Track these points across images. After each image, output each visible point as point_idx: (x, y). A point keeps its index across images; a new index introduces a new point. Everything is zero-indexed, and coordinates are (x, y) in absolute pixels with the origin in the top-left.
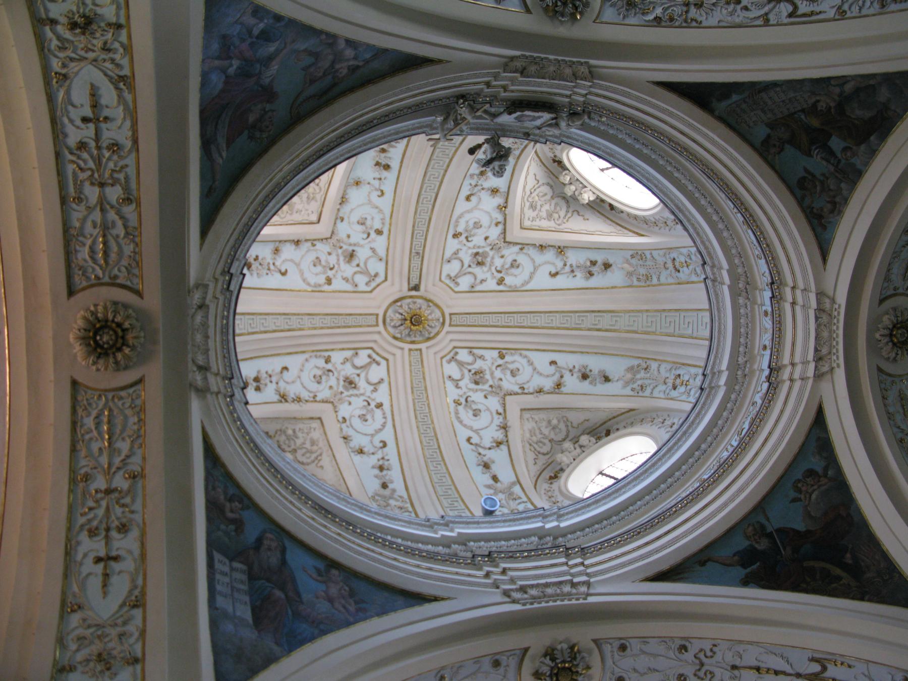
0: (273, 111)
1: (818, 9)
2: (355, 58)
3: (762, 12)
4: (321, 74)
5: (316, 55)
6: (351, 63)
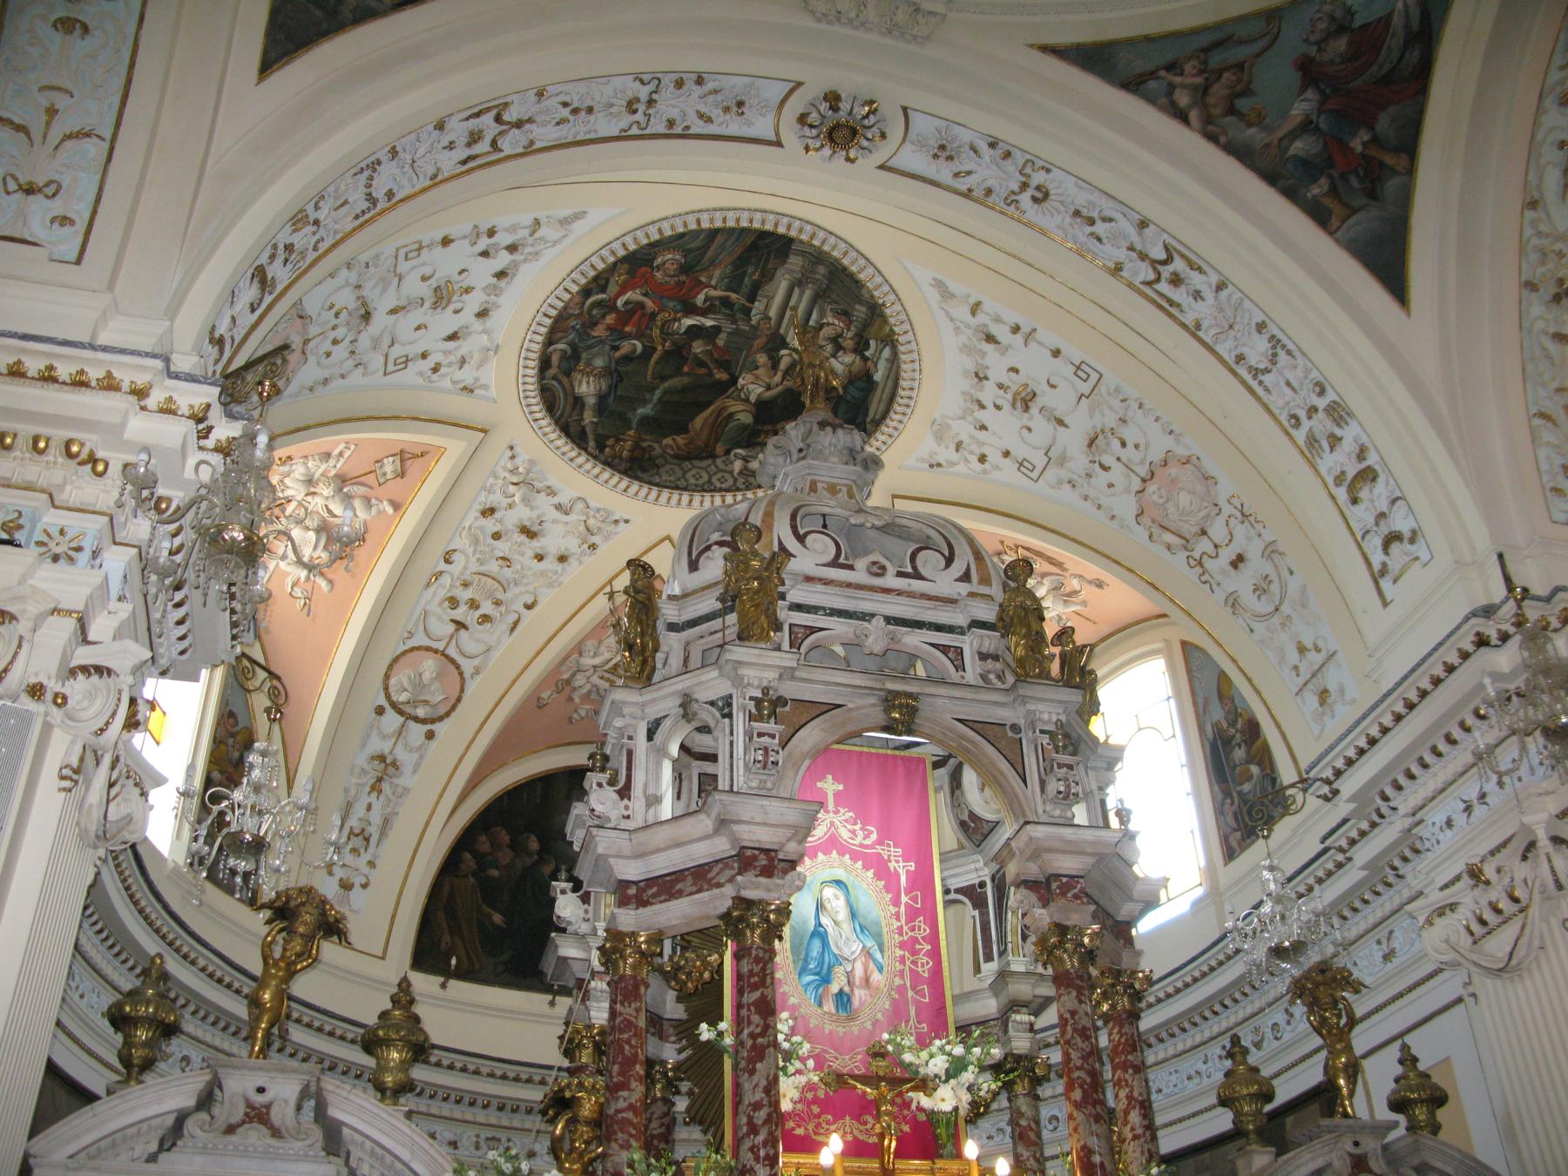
0: (1306, 40)
1: (473, 122)
2: (1171, 88)
3: (546, 103)
4: (1226, 75)
5: (1231, 110)
6: (1178, 80)
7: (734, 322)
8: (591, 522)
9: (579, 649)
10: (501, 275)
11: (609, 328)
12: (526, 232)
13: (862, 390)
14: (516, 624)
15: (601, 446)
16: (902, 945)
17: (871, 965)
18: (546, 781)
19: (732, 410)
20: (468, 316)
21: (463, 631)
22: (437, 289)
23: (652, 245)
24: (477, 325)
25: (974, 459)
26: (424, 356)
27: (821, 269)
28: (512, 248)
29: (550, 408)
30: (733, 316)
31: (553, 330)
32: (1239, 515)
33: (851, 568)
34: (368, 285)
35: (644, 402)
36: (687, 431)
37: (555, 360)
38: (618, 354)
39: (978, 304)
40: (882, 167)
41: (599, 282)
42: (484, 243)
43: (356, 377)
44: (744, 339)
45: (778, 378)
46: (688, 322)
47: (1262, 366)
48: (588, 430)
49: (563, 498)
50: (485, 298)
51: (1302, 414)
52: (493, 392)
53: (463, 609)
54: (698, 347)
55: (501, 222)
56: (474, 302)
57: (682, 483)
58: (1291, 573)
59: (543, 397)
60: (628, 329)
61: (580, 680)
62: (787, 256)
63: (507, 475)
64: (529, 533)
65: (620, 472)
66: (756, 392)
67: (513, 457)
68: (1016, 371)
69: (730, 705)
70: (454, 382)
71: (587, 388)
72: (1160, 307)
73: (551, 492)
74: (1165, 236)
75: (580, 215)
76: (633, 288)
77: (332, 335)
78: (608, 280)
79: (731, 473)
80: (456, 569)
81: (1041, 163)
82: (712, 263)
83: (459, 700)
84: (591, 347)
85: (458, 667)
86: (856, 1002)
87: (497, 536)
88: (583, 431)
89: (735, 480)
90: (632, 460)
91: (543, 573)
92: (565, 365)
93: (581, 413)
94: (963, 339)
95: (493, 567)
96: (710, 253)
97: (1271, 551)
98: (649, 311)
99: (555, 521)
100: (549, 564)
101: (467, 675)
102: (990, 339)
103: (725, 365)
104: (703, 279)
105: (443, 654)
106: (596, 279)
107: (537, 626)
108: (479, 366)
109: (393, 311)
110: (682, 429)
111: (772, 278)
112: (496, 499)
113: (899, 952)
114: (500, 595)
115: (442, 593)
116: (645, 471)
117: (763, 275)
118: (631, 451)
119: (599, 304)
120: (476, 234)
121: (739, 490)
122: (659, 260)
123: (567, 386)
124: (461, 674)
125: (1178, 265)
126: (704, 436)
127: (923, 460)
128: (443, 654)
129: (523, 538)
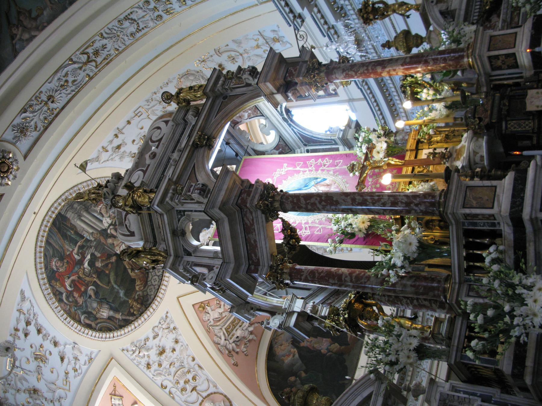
2: (20, 39)
4: (21, 18)
5: (35, 19)
6: (18, 36)
7: (91, 247)
8: (164, 326)
9: (217, 344)
10: (39, 331)
11: (80, 296)
12: (22, 316)
14: (200, 367)
15: (133, 315)
16: (317, 170)
17: (322, 183)
18: (270, 370)
20: (55, 351)
21: (197, 388)
22: (36, 359)
23: (46, 268)
24: (61, 348)
26: (67, 374)
27: (76, 206)
28: (28, 323)
29: (110, 330)
31: (74, 319)
32: (203, 63)
35: (118, 292)
37: (88, 322)
38: (93, 296)
39: (103, 148)
40: (25, 157)
41: (57, 294)
42: (21, 334)
44: (99, 246)
46: (86, 265)
47: (136, 26)
48: (124, 318)
49: (151, 336)
50: (48, 341)
51: (156, 14)
52: (95, 351)
53: (187, 386)
54: (99, 264)
55: (13, 323)
56: (48, 345)
57: (157, 287)
58: (228, 45)
59: (104, 332)
60: (83, 289)
61: (230, 347)
62: (66, 218)
63: (135, 355)
64: (162, 352)
65: (145, 310)
67: (127, 351)
68: (134, 141)
69: (180, 211)
70: (85, 364)
71: (105, 313)
72: (108, 64)
73: (147, 339)
74: (78, 53)
75: (22, 293)
76: (64, 282)
78: (57, 290)
80: (169, 385)
81: (37, 94)
82: (62, 248)
83: (225, 396)
84: (87, 306)
85: (212, 394)
87: (160, 365)
88: (125, 320)
90: (142, 304)
91: (181, 351)
92: (92, 319)
93: (116, 319)
94: (117, 158)
95: (173, 370)
96: (57, 247)
97: (218, 52)
98: (76, 278)
99: (160, 341)
100: (178, 347)
101: (216, 391)
102: (119, 147)
103: (109, 256)
104: (68, 253)
105: (204, 398)
106: (54, 294)
107: (202, 358)
108: (81, 352)
110: (133, 281)
111: (75, 227)
112: (144, 362)
113: (320, 171)
114: (186, 370)
115: (178, 393)
116: (148, 300)
117: (72, 229)
118: (138, 303)
119: (67, 298)
122: (54, 268)
123: (102, 320)
124: (215, 393)
125: (90, 50)
128: (204, 398)
129: (164, 355)
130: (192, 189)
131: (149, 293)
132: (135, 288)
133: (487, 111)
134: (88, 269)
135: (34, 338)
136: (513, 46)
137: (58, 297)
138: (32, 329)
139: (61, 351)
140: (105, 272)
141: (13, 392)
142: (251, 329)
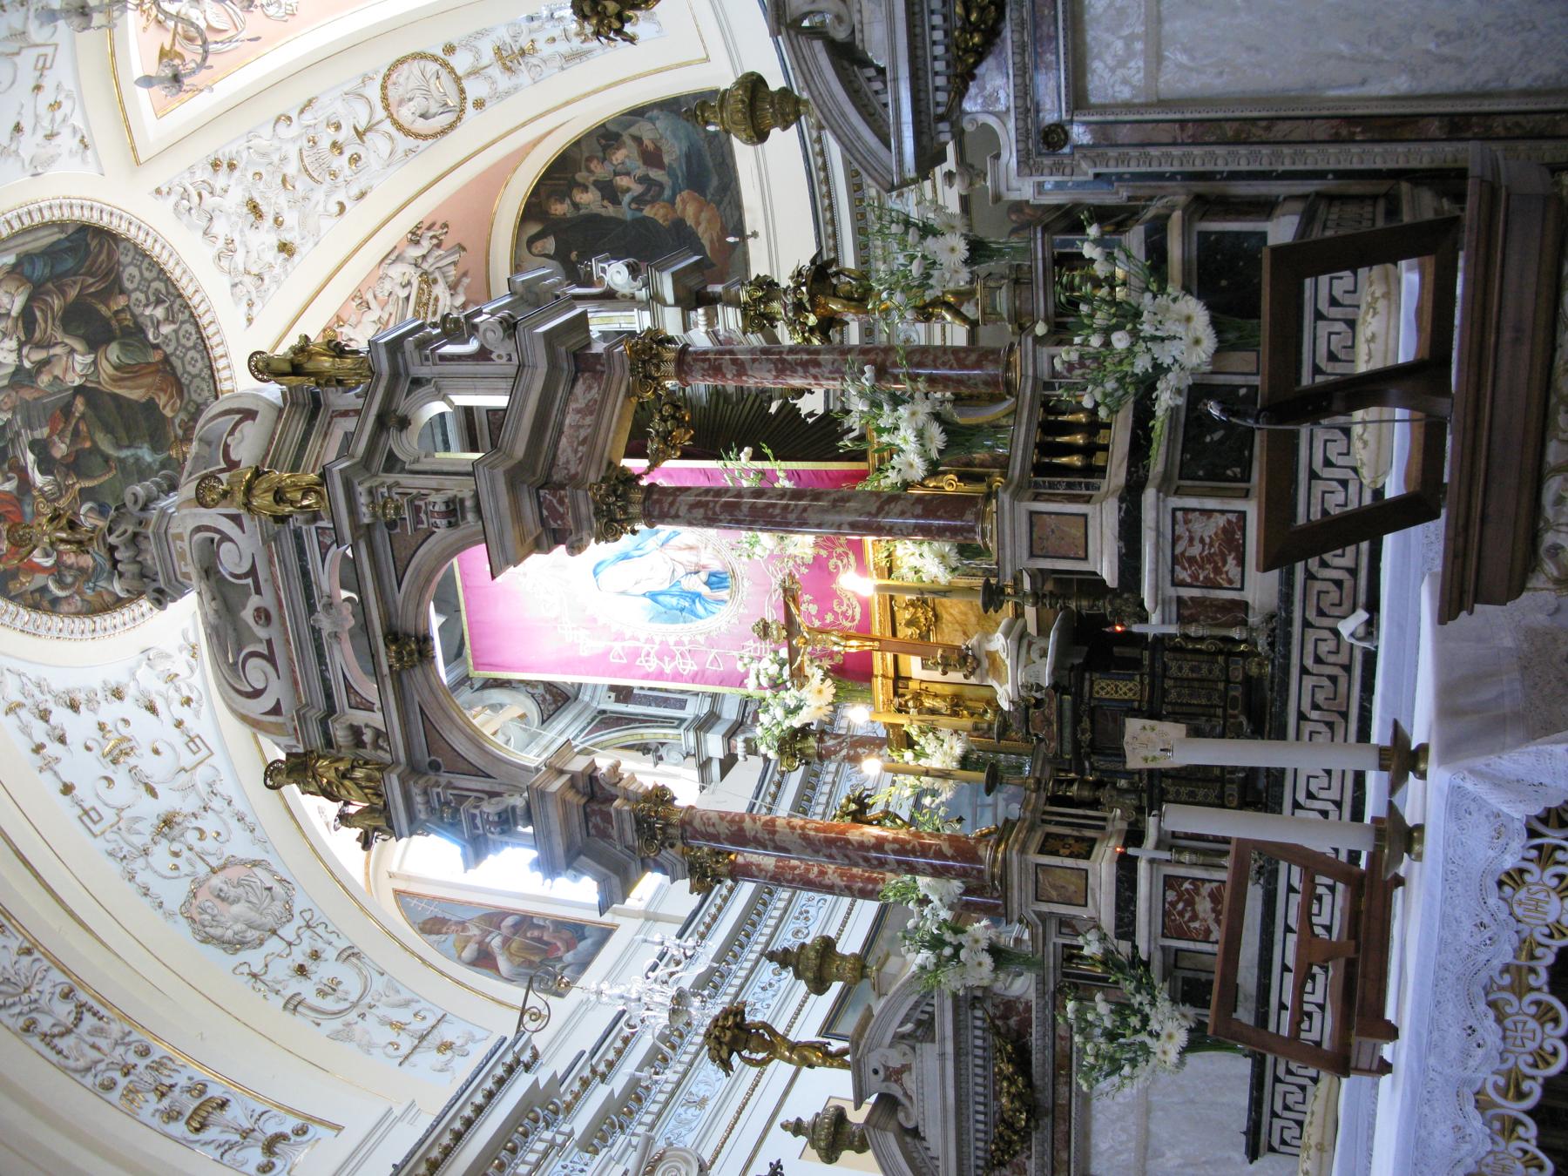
7: (18, 434)
10: (74, 706)
12: (23, 713)
13: (33, 264)
19: (110, 371)
20: (128, 708)
22: (115, 762)
24: (131, 692)
25: (59, 115)
26: (179, 724)
28: (44, 715)
30: (12, 440)
33: (269, 642)
34: (138, 841)
35: (138, 460)
36: (151, 400)
42: (53, 749)
43: (227, 787)
45: (58, 350)
46: (39, 479)
54: (60, 449)
55: (23, 747)
56: (110, 712)
66: (81, 360)
70: (192, 670)
77: (198, 845)
79: (176, 331)
86: (716, 566)
89: (183, 322)
103: (67, 410)
106: (36, 607)
108: (168, 656)
109: (152, 792)
110: (150, 406)
119: (61, 583)
120: (49, 766)
121: (192, 315)
126: (149, 380)
127: (84, 161)
130: (478, 821)
131: (200, 400)
132: (163, 416)
133: (1051, 724)
134: (49, 483)
135: (80, 727)
136: (1081, 554)
137: (45, 604)
138: (60, 715)
139: (138, 694)
140: (83, 450)
141: (141, 862)
142: (460, 300)
